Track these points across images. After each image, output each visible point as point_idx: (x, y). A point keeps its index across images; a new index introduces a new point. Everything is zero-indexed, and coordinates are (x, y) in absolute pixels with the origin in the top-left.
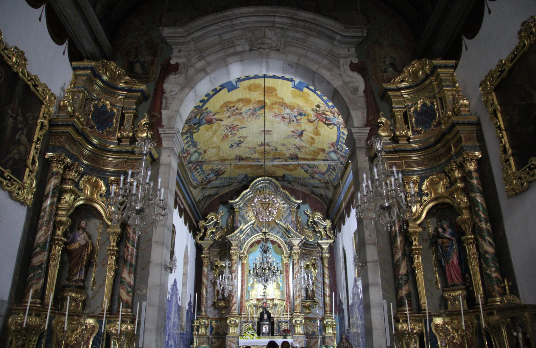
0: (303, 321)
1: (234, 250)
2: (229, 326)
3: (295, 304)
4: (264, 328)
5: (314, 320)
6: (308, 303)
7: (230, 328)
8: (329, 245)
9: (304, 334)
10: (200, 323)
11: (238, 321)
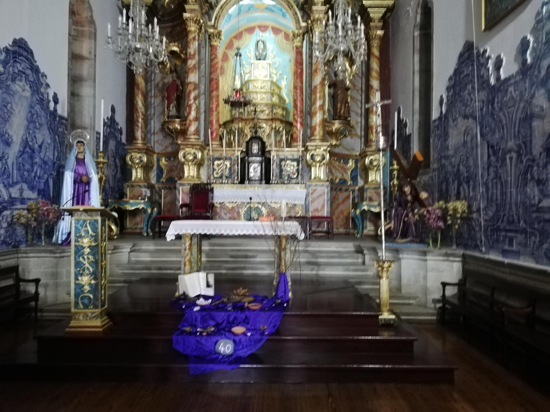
0: (328, 156)
1: (192, 11)
2: (183, 164)
3: (313, 124)
4: (251, 170)
5: (345, 158)
6: (337, 125)
7: (186, 168)
8: (383, 10)
9: (328, 181)
10: (131, 159)
11: (199, 155)
